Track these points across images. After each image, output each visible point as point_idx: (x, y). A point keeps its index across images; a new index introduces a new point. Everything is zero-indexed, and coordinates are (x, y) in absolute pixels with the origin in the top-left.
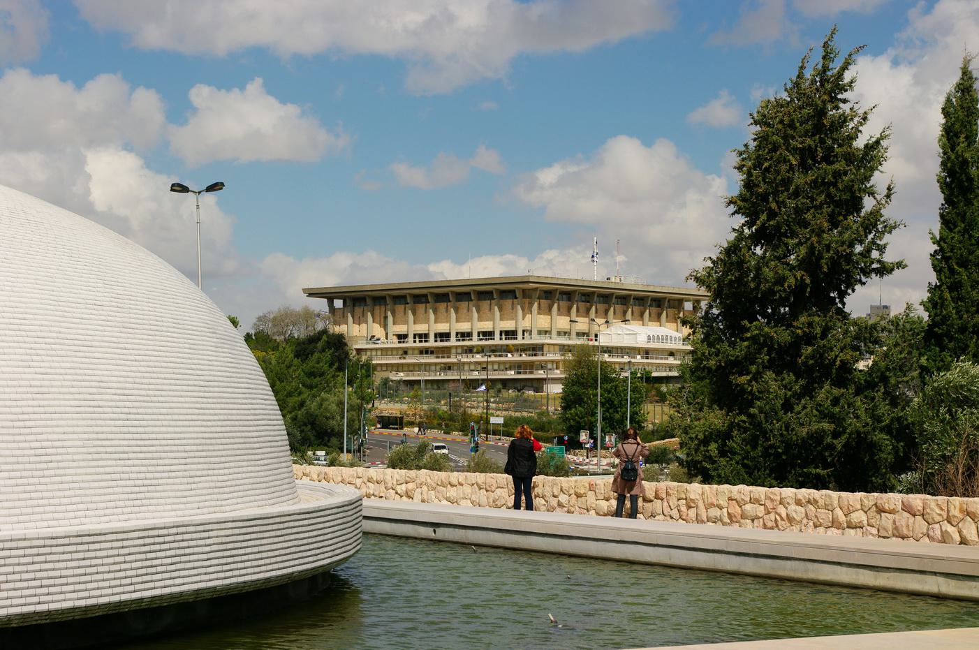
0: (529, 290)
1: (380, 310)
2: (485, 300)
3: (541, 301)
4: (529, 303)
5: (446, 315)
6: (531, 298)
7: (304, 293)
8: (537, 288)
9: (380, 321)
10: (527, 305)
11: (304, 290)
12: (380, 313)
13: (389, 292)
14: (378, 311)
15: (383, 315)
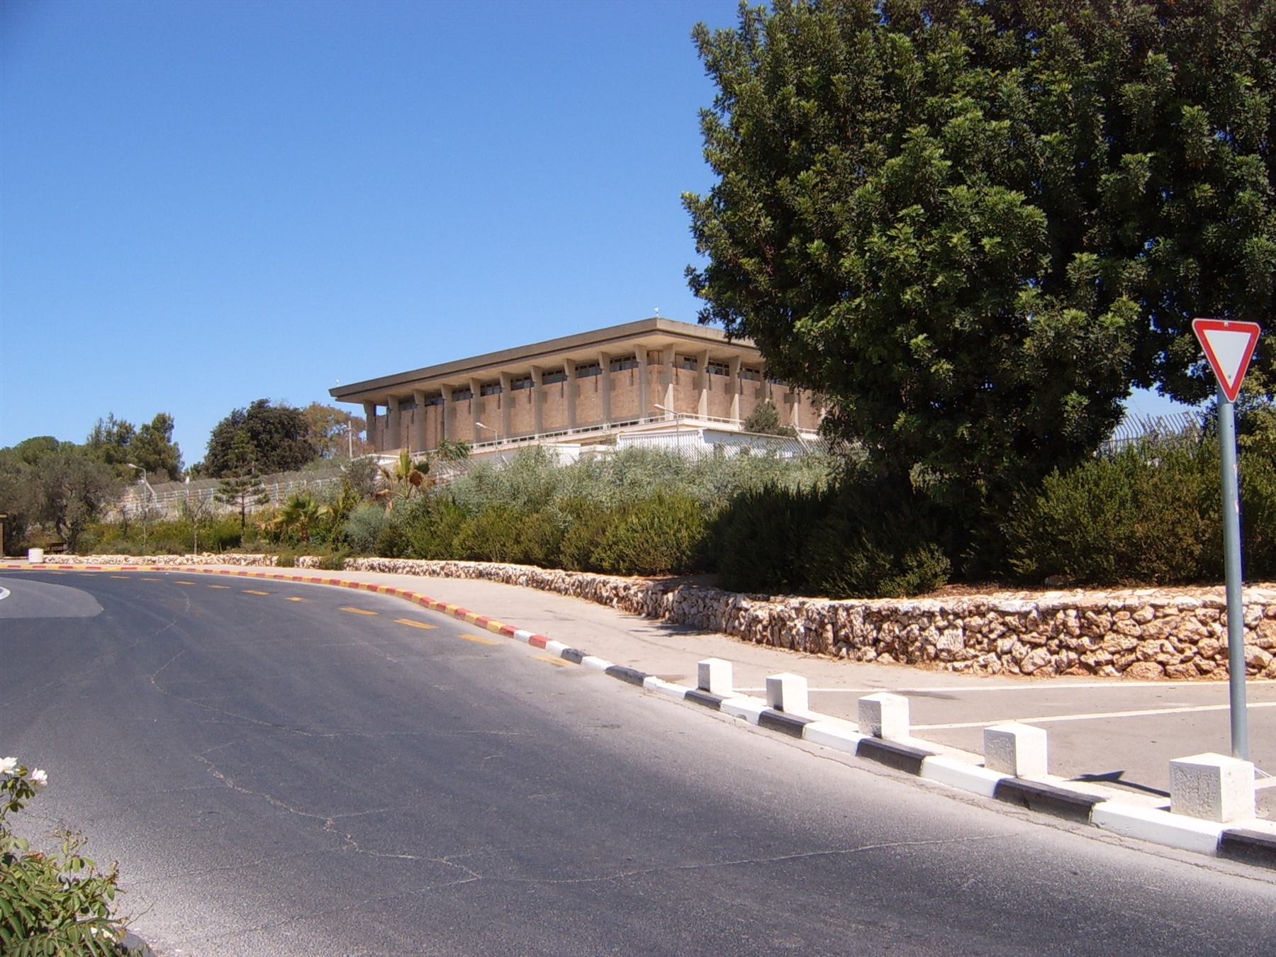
0: (659, 351)
1: (436, 412)
2: (587, 375)
3: (679, 370)
4: (660, 372)
5: (528, 406)
6: (662, 364)
7: (332, 395)
8: (670, 346)
9: (436, 428)
10: (655, 376)
11: (334, 392)
12: (436, 416)
13: (418, 386)
14: (433, 413)
15: (440, 420)
